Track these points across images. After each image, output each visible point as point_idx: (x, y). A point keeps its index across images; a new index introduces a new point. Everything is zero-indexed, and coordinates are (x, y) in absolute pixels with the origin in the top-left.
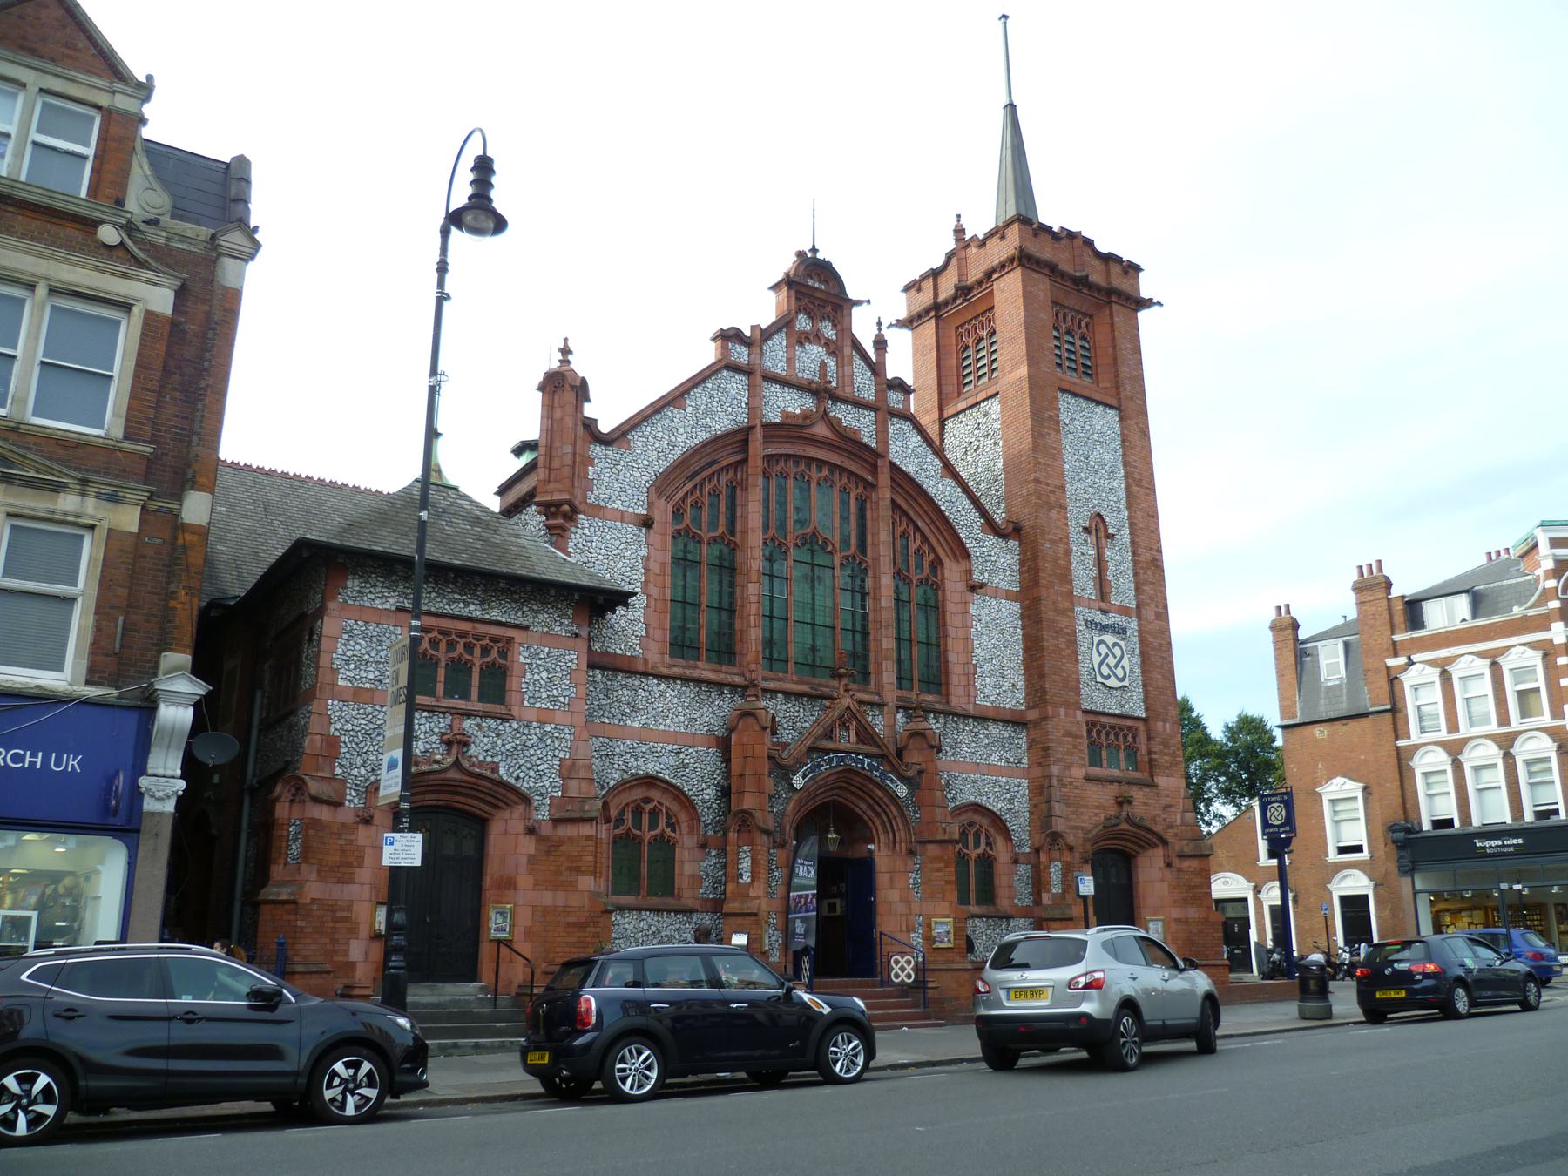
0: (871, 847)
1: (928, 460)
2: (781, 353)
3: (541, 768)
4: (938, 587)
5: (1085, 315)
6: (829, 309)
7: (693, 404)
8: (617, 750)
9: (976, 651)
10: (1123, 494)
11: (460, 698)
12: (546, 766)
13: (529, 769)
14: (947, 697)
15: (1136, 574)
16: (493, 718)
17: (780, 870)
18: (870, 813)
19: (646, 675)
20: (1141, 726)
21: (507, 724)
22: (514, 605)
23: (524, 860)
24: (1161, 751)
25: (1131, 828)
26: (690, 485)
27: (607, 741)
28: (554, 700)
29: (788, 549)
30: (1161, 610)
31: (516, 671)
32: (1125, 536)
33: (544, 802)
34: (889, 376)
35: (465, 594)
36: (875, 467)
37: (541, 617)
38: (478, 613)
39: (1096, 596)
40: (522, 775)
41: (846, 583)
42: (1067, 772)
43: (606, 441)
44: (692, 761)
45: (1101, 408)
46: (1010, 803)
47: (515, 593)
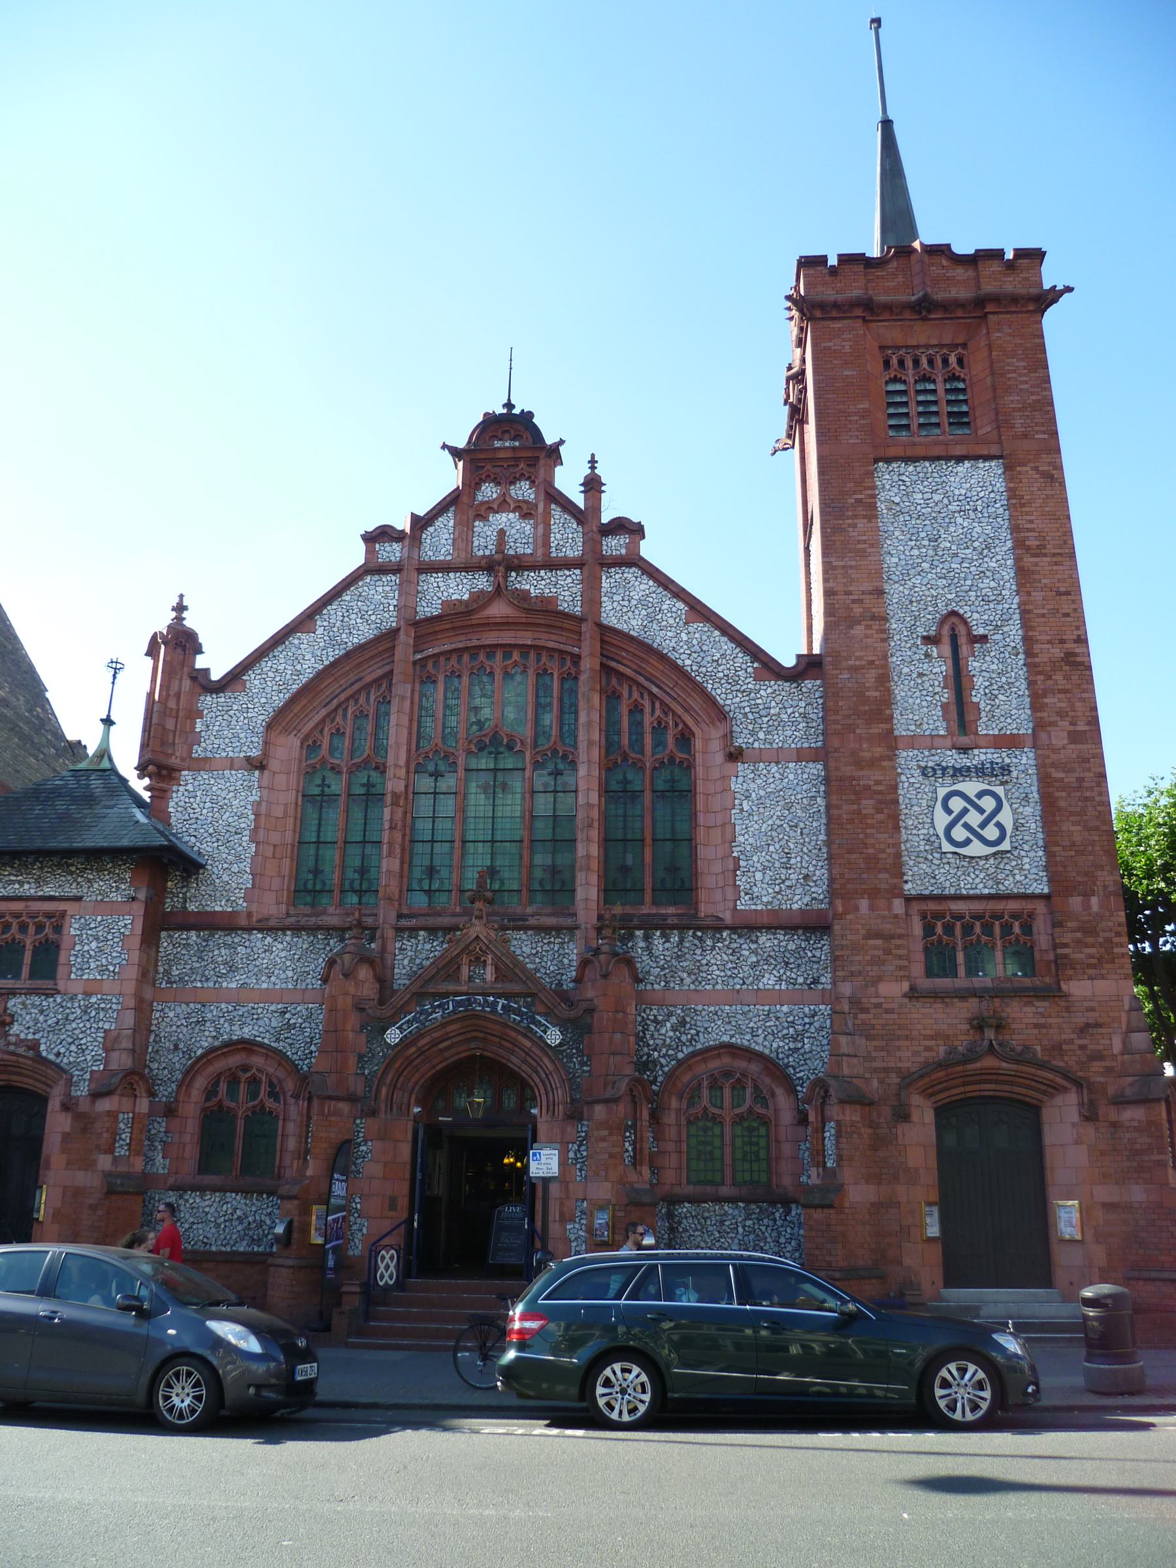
0: (534, 1111)
1: (665, 607)
2: (447, 536)
3: (83, 1041)
4: (688, 766)
5: (953, 346)
6: (522, 466)
7: (325, 624)
8: (209, 1016)
9: (741, 839)
10: (1008, 574)
11: (13, 978)
12: (89, 1039)
13: (70, 1044)
14: (695, 905)
15: (1031, 684)
16: (37, 994)
17: (370, 1143)
18: (524, 1067)
19: (249, 929)
20: (1040, 907)
21: (51, 1000)
22: (69, 878)
23: (57, 1138)
24: (1079, 942)
25: (1004, 1065)
26: (324, 712)
27: (199, 1006)
28: (102, 970)
29: (456, 757)
30: (1081, 727)
31: (64, 945)
32: (1014, 631)
33: (84, 1077)
34: (606, 518)
35: (21, 875)
36: (580, 633)
37: (96, 885)
38: (32, 891)
39: (948, 729)
40: (62, 1050)
41: (545, 785)
42: (871, 990)
43: (220, 687)
44: (300, 1020)
45: (967, 464)
46: (795, 1040)
47: (72, 865)
